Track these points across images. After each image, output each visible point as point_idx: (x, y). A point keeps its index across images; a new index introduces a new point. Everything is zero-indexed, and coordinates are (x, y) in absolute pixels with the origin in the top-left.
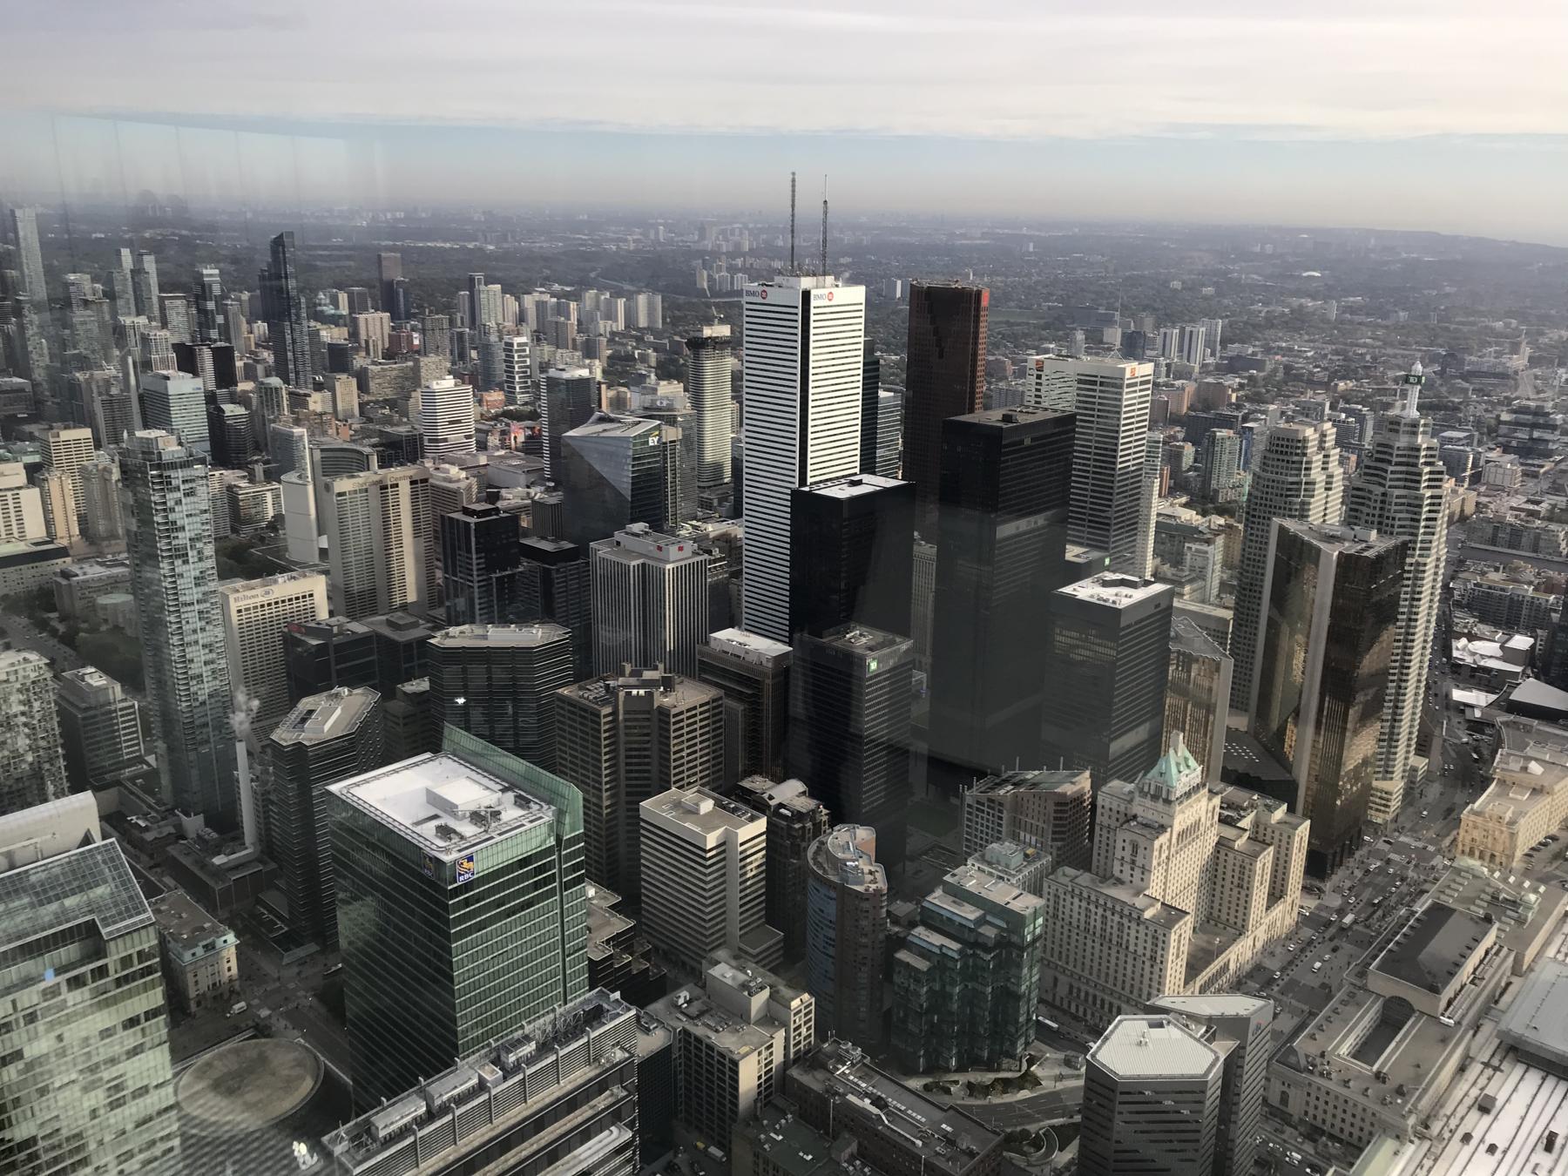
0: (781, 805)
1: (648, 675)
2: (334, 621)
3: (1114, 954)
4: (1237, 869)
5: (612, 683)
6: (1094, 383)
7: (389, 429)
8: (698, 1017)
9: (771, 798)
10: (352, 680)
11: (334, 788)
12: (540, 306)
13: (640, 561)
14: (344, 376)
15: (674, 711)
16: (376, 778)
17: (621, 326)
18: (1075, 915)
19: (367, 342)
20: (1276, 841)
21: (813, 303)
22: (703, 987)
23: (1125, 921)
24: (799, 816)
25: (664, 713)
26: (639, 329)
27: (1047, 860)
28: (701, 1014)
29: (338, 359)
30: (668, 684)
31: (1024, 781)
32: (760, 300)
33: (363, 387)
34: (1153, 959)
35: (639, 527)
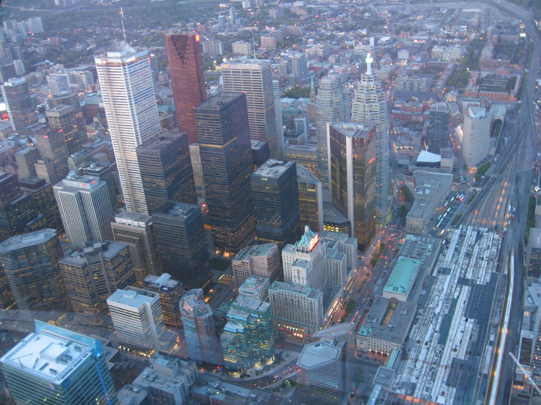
0: (163, 286)
3: (298, 310)
4: (335, 266)
6: (249, 73)
8: (153, 381)
9: (158, 284)
18: (282, 301)
20: (346, 251)
22: (152, 368)
23: (300, 299)
24: (170, 289)
27: (267, 280)
28: (154, 378)
30: (105, 248)
31: (254, 251)
34: (311, 310)
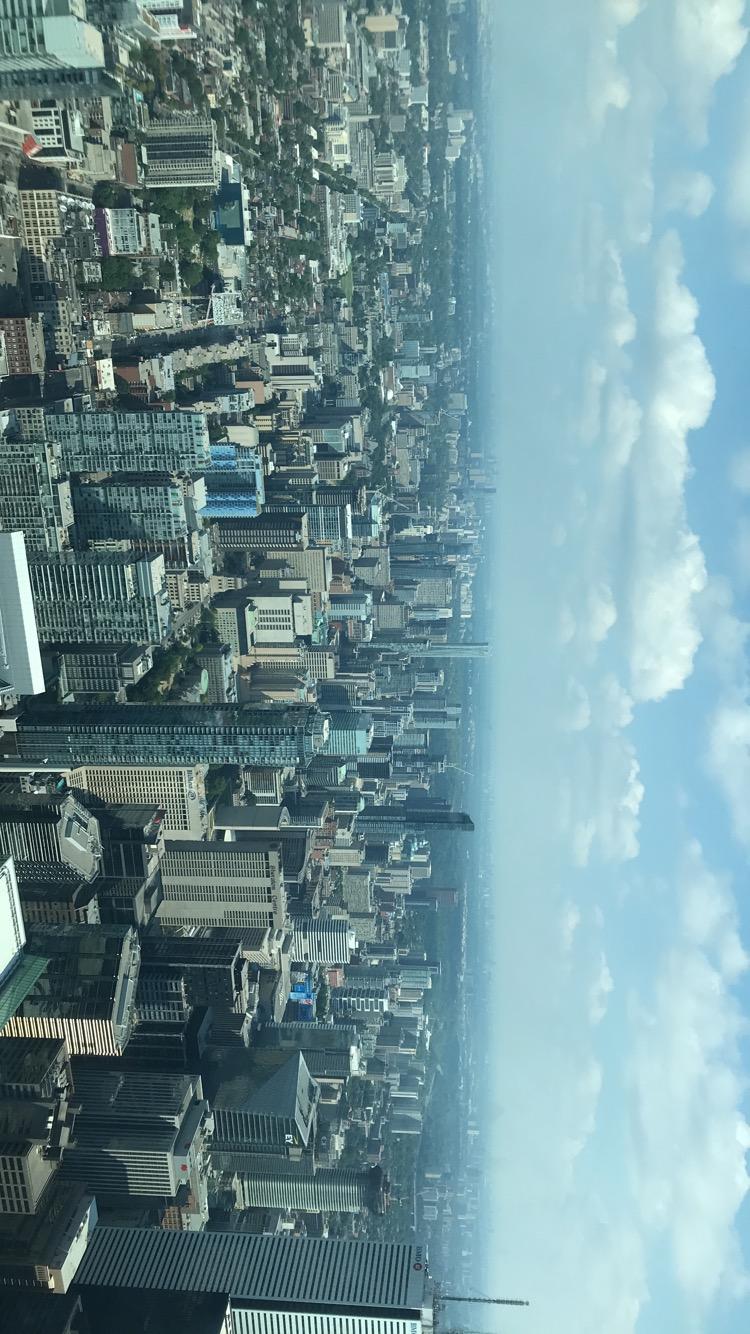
1: (65, 1132)
2: (162, 844)
5: (63, 1096)
7: (317, 891)
10: (109, 862)
11: (10, 864)
12: (413, 1022)
13: (178, 1125)
14: (362, 856)
15: (22, 1159)
16: (11, 897)
17: (395, 1094)
19: (389, 875)
21: (408, 1323)
25: (24, 1149)
26: (391, 1108)
29: (376, 853)
30: (50, 1154)
32: (413, 1262)
33: (352, 871)
35: (210, 1124)
